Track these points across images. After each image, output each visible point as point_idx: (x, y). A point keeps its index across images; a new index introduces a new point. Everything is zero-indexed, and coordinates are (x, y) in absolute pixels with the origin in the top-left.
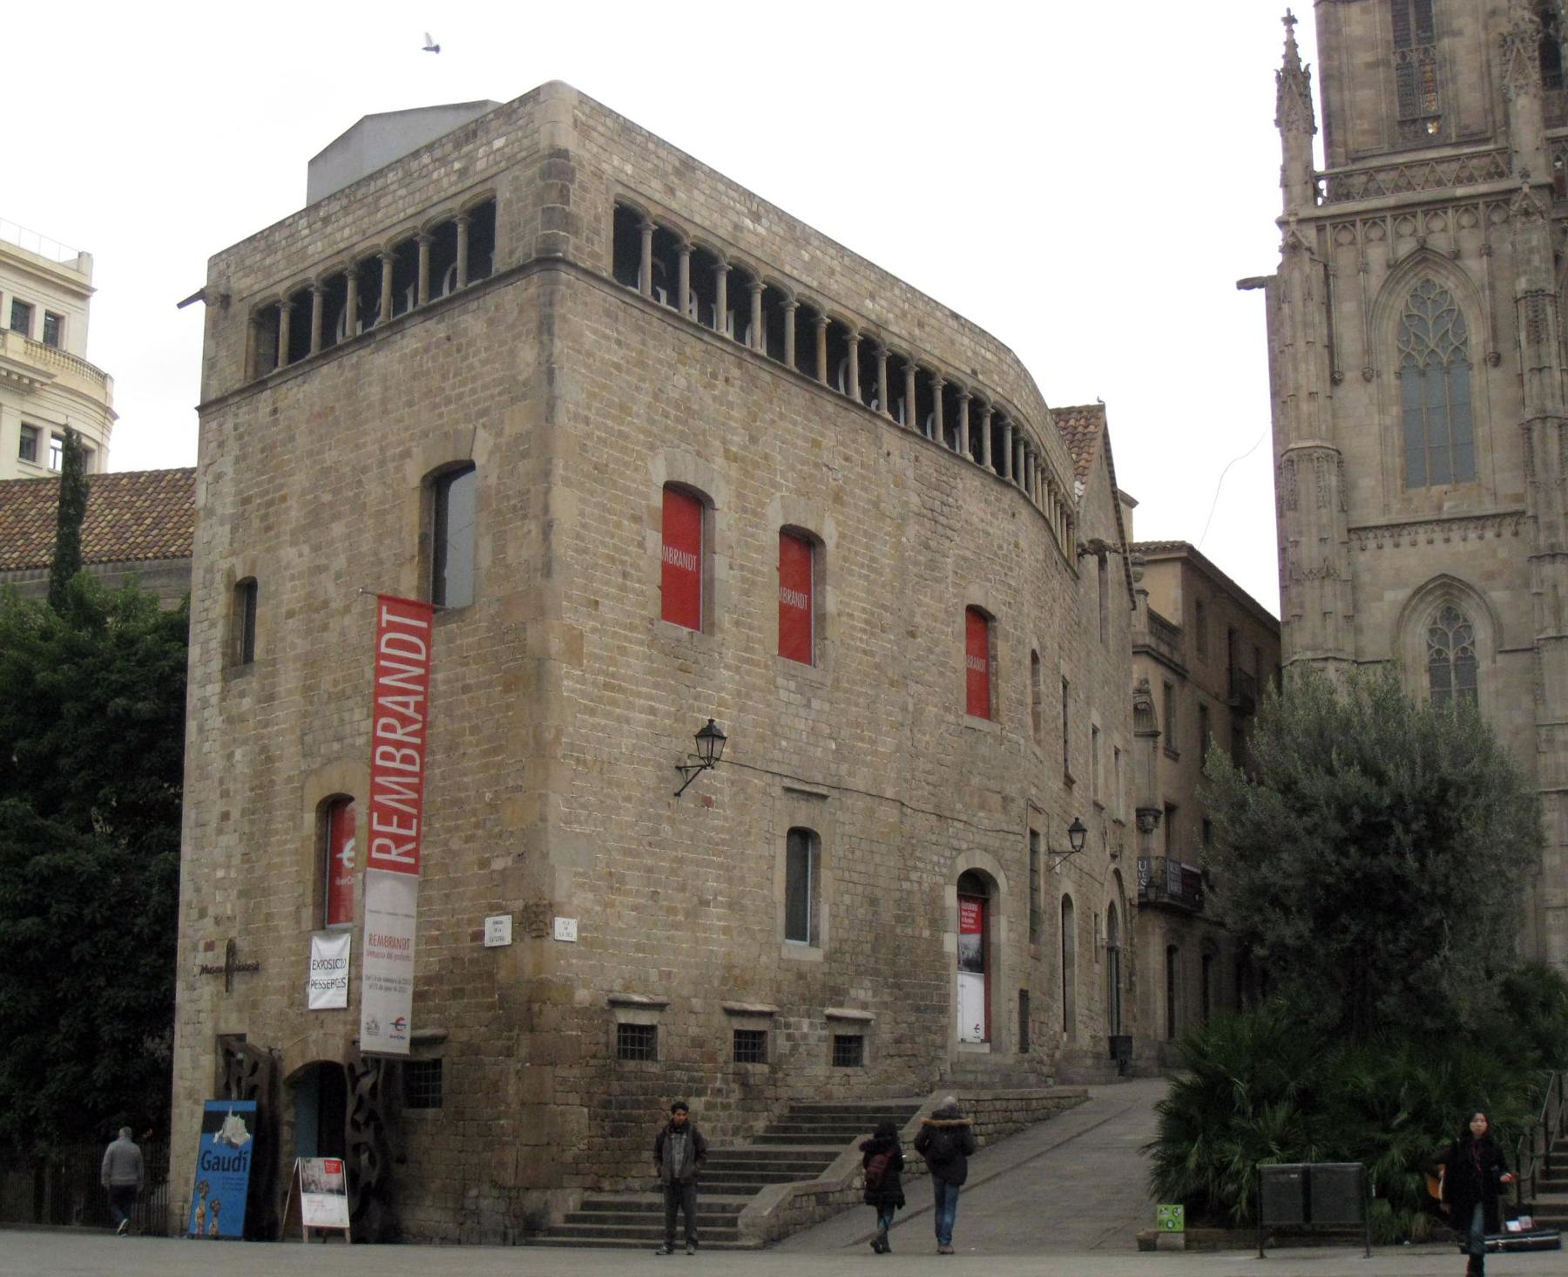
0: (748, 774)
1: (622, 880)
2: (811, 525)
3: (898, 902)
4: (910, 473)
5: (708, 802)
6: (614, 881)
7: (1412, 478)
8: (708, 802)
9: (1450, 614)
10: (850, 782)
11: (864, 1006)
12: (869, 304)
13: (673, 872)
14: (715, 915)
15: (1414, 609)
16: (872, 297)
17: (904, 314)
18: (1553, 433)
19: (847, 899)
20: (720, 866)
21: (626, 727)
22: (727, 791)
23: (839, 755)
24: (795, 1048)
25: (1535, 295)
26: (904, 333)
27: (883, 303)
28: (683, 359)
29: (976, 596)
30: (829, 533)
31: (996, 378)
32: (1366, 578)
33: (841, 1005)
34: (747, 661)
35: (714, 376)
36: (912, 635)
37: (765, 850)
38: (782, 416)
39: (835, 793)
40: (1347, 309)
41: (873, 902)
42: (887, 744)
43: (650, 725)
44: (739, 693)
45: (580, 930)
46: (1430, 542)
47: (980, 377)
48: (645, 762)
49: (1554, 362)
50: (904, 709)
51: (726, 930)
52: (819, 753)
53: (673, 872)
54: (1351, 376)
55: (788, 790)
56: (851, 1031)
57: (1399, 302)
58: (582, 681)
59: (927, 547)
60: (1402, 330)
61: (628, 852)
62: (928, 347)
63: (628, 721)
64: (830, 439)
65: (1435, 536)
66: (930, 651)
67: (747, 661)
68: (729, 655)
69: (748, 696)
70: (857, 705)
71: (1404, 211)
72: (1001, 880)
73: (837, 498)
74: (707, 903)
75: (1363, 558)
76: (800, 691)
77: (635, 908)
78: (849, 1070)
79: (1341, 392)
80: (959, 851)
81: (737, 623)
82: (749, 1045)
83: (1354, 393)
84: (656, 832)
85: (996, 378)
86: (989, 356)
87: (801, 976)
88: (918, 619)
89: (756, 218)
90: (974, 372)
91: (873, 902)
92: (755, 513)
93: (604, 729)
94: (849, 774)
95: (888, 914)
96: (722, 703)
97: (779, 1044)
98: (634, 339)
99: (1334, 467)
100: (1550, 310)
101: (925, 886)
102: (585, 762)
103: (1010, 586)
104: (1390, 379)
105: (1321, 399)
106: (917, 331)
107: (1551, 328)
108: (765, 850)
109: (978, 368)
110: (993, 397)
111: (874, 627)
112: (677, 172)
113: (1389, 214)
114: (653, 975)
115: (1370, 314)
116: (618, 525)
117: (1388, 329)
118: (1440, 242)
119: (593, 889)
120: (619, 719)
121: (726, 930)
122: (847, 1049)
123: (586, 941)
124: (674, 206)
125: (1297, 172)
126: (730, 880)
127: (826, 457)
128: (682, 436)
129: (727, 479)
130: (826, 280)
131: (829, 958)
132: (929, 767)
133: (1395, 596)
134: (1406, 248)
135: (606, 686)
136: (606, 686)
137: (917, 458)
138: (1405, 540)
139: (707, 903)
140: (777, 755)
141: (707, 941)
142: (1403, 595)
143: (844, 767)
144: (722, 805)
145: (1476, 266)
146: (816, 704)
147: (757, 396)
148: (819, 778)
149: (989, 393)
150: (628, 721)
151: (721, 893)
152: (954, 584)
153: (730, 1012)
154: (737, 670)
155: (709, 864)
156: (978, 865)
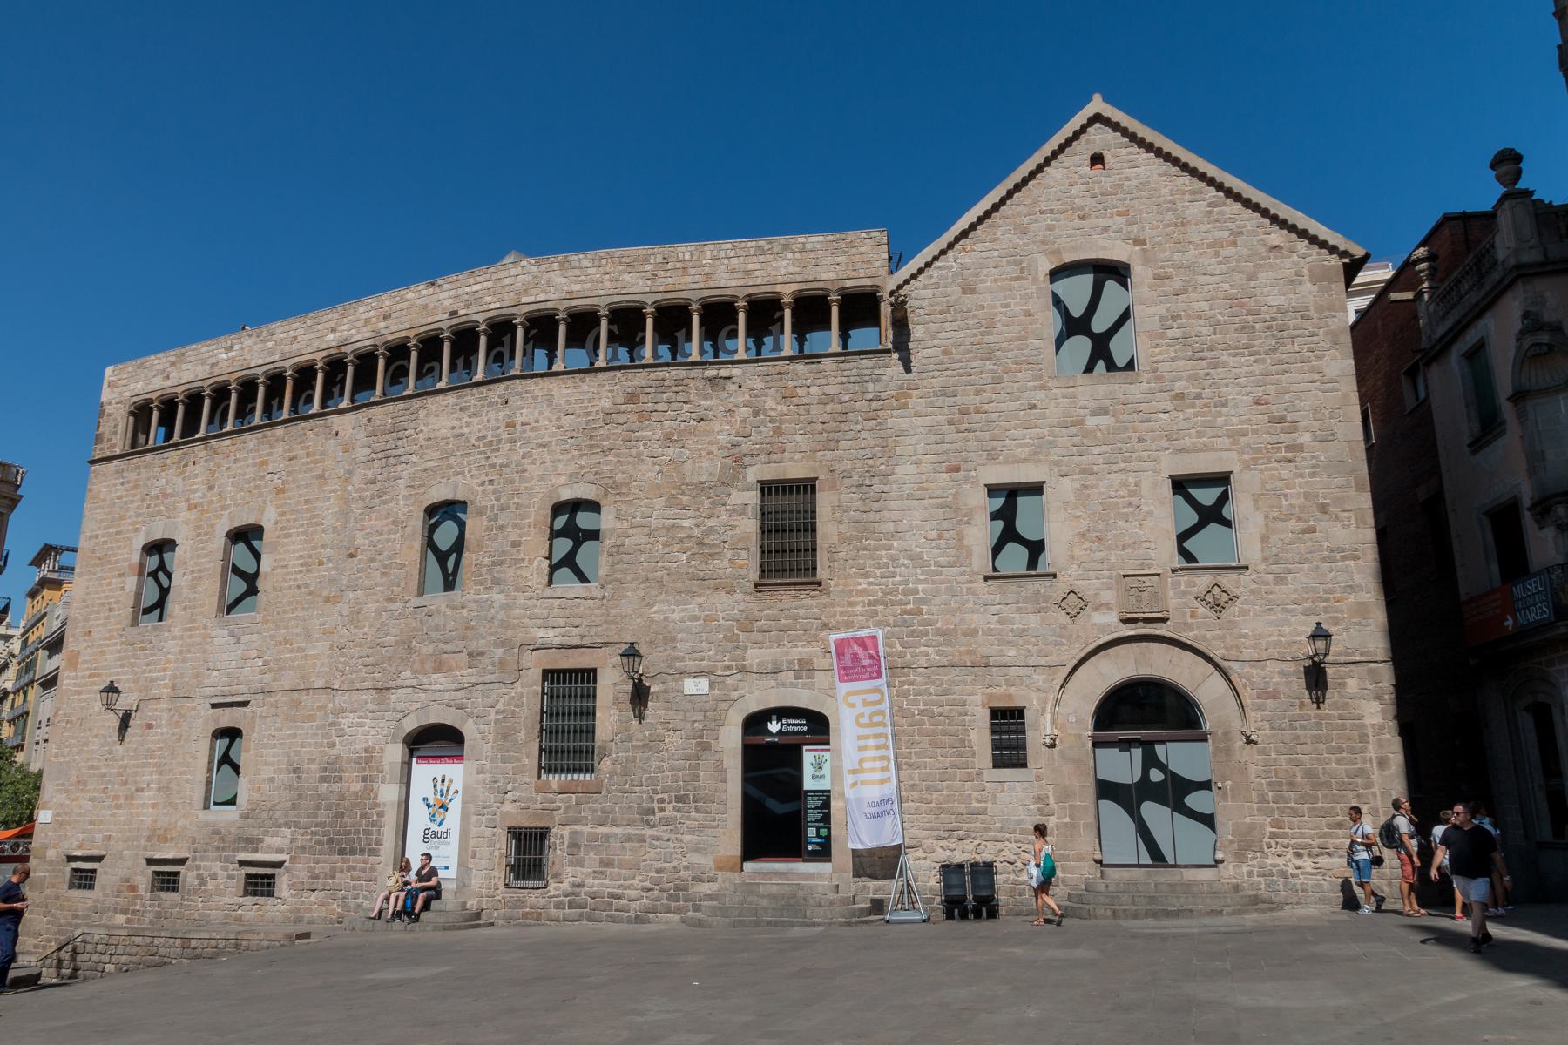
0: (178, 703)
1: (85, 784)
2: (251, 521)
4: (361, 436)
8: (150, 726)
11: (280, 851)
13: (119, 774)
14: (148, 797)
16: (333, 330)
17: (368, 321)
20: (155, 765)
24: (203, 884)
28: (164, 467)
29: (439, 493)
31: (488, 299)
33: (256, 850)
34: (190, 630)
35: (186, 465)
36: (352, 556)
38: (236, 461)
39: (261, 696)
44: (181, 652)
45: (54, 816)
47: (461, 312)
51: (154, 806)
53: (119, 774)
55: (214, 706)
56: (262, 871)
58: (76, 677)
59: (373, 482)
61: (93, 767)
64: (279, 449)
66: (372, 560)
67: (190, 630)
68: (176, 631)
69: (189, 651)
70: (286, 628)
76: (232, 634)
77: (91, 799)
78: (261, 900)
81: (185, 608)
82: (167, 881)
84: (111, 752)
85: (488, 299)
87: (216, 832)
88: (359, 541)
89: (230, 348)
90: (454, 314)
92: (206, 534)
94: (275, 680)
96: (169, 662)
97: (188, 876)
98: (132, 476)
103: (493, 466)
106: (382, 324)
110: (480, 318)
111: (307, 566)
112: (173, 364)
114: (99, 837)
116: (109, 584)
119: (67, 791)
121: (154, 806)
122: (260, 883)
126: (161, 773)
130: (286, 348)
131: (245, 817)
135: (90, 676)
136: (90, 676)
141: (138, 814)
144: (160, 726)
146: (244, 639)
148: (243, 689)
149: (475, 318)
152: (405, 498)
153: (150, 861)
154: (181, 638)
155: (146, 765)
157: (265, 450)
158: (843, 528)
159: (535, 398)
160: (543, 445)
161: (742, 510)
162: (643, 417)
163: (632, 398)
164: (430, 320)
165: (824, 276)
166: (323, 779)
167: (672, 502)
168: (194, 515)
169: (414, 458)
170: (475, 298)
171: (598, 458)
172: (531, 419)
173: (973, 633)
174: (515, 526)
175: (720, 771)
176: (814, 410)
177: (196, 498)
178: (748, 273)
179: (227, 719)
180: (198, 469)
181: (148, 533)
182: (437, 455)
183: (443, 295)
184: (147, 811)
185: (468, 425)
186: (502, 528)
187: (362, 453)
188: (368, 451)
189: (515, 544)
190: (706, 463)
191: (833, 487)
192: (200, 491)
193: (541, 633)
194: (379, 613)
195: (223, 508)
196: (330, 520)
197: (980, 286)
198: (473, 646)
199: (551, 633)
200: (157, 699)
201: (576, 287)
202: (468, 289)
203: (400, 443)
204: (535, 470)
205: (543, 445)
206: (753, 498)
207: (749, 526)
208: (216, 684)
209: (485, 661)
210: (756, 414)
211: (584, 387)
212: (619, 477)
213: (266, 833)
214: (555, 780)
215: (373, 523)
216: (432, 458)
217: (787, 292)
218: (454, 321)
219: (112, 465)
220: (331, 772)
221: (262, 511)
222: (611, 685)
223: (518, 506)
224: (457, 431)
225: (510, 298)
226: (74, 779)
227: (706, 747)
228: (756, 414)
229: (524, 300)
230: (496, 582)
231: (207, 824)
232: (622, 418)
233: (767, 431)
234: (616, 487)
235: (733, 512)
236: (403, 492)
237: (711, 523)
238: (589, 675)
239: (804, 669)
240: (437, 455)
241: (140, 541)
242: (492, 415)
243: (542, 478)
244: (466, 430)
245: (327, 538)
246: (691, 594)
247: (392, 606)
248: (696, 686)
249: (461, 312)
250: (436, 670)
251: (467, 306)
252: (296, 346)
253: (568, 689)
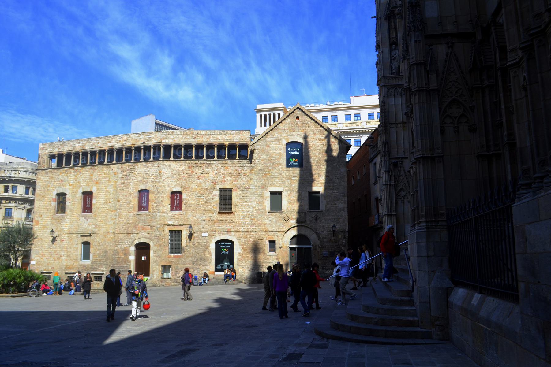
0: (71, 235)
2: (89, 190)
3: (113, 252)
4: (120, 171)
6: (43, 255)
8: (63, 241)
10: (99, 232)
11: (103, 271)
12: (109, 144)
14: (64, 258)
16: (110, 142)
17: (120, 141)
19: (98, 252)
22: (67, 238)
23: (96, 227)
28: (61, 173)
30: (94, 190)
37: (76, 246)
41: (106, 252)
42: (110, 223)
50: (116, 215)
52: (90, 228)
59: (124, 183)
64: (96, 172)
68: (68, 217)
72: (151, 244)
73: (97, 183)
76: (85, 218)
80: (135, 239)
87: (84, 266)
88: (120, 197)
89: (79, 143)
90: (144, 142)
91: (106, 252)
95: (110, 253)
98: (51, 175)
101: (123, 247)
106: (124, 143)
108: (76, 246)
109: (145, 141)
110: (151, 144)
111: (106, 202)
112: (61, 145)
114: (50, 268)
123: (38, 264)
124: (60, 150)
127: (94, 177)
128: (60, 186)
129: (69, 189)
130: (96, 145)
132: (124, 224)
143: (97, 230)
146: (89, 220)
147: (77, 172)
153: (66, 273)
156: (142, 241)
157: (92, 172)
158: (238, 200)
160: (168, 178)
161: (215, 195)
162: (192, 172)
163: (190, 167)
165: (235, 141)
166: (114, 254)
167: (199, 192)
168: (71, 187)
169: (134, 178)
170: (150, 139)
171: (182, 181)
172: (165, 171)
173: (265, 224)
174: (162, 197)
175: (210, 253)
176: (233, 172)
177: (72, 182)
178: (217, 138)
179: (85, 239)
180: (71, 175)
181: (57, 191)
182: (141, 178)
184: (64, 261)
186: (159, 197)
187: (120, 175)
189: (162, 201)
190: (207, 184)
191: (236, 191)
192: (75, 181)
193: (169, 222)
194: (127, 216)
195: (80, 186)
196: (112, 191)
197: (271, 146)
198: (152, 224)
199: (171, 222)
200: (65, 234)
201: (176, 139)
204: (166, 184)
205: (168, 178)
206: (218, 192)
207: (217, 199)
208: (82, 230)
209: (155, 228)
210: (219, 173)
211: (178, 164)
212: (187, 186)
213: (99, 267)
214: (172, 255)
215: (124, 193)
216: (140, 178)
217: (227, 144)
219: (44, 171)
220: (116, 253)
221: (92, 188)
222: (185, 234)
223: (162, 192)
225: (159, 140)
226: (41, 253)
227: (207, 248)
228: (219, 173)
230: (158, 210)
231: (81, 265)
232: (188, 172)
233: (221, 176)
234: (186, 188)
235: (214, 195)
236: (132, 186)
237: (209, 198)
238: (180, 232)
239: (229, 231)
240: (141, 178)
241: (55, 192)
242: (155, 169)
243: (168, 186)
245: (111, 196)
246: (204, 214)
247: (130, 214)
248: (205, 235)
250: (142, 230)
251: (148, 141)
252: (99, 145)
253: (176, 234)
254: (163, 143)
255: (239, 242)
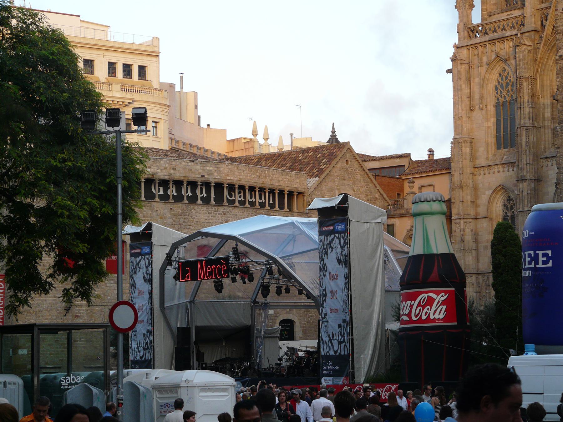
4: (168, 215)
5: (77, 316)
7: (498, 147)
8: (77, 316)
9: (509, 199)
15: (495, 198)
17: (166, 168)
18: (524, 133)
21: (45, 302)
25: (521, 78)
26: (165, 174)
27: (155, 168)
32: (481, 186)
40: (476, 81)
43: (54, 300)
46: (499, 172)
47: (206, 176)
48: (52, 310)
49: (526, 105)
51: (84, 347)
54: (477, 107)
57: (494, 77)
60: (496, 88)
62: (178, 174)
63: (46, 300)
65: (500, 169)
71: (492, 41)
74: (77, 341)
75: (480, 178)
79: (474, 114)
83: (478, 115)
85: (216, 174)
86: (211, 169)
90: (203, 176)
93: (37, 304)
99: (468, 144)
100: (525, 84)
102: (30, 313)
104: (492, 109)
105: (464, 118)
106: (172, 171)
107: (525, 91)
113: (487, 43)
115: (482, 84)
117: (491, 87)
118: (503, 53)
120: (42, 301)
121: (84, 347)
125: (462, 26)
133: (489, 193)
134: (493, 56)
137: (171, 209)
138: (491, 171)
139: (77, 341)
140: (107, 301)
142: (491, 191)
144: (83, 317)
145: (513, 62)
150: (46, 300)
151: (82, 338)
159: (233, 215)
164: (193, 176)
165: (295, 186)
170: (210, 173)
178: (279, 181)
183: (198, 167)
185: (211, 219)
188: (172, 221)
201: (241, 177)
202: (208, 168)
203: (185, 220)
211: (245, 213)
218: (203, 179)
224: (207, 221)
229: (228, 178)
242: (221, 218)
244: (211, 221)
249: (206, 176)
251: (208, 174)
254: (228, 182)
255: (300, 323)
